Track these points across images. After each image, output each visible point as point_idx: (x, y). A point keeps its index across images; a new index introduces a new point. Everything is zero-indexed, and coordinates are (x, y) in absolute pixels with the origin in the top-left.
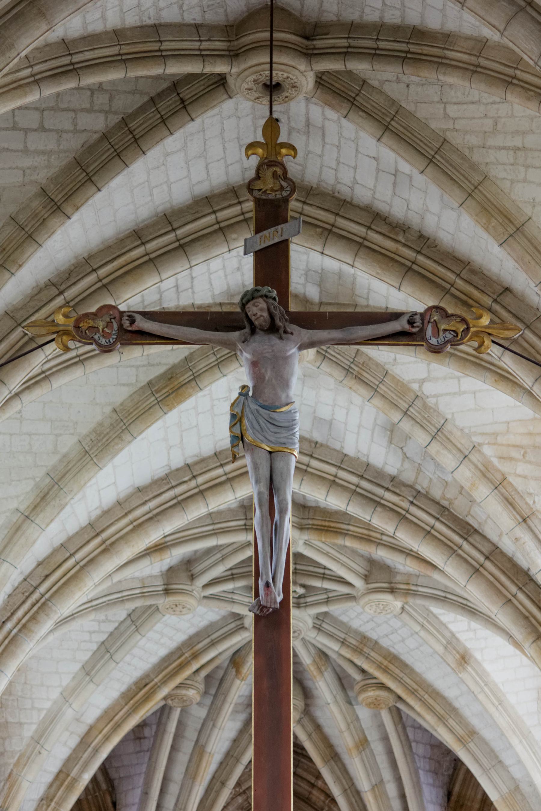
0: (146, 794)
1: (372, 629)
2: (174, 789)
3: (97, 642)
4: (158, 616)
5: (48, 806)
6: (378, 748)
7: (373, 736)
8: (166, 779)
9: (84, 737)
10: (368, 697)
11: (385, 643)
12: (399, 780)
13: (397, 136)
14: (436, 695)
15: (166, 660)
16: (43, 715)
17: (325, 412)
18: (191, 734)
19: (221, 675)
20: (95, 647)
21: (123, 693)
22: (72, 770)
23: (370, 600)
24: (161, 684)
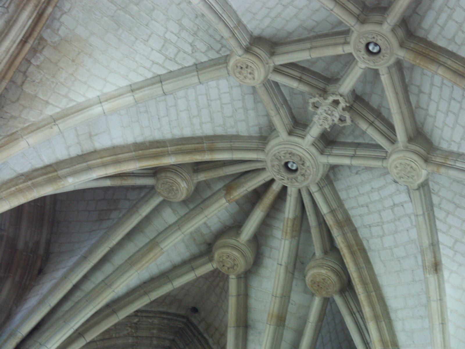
1: (361, 216)
2: (108, 269)
3: (154, 73)
4: (224, 72)
5: (24, 182)
9: (85, 154)
10: (319, 274)
11: (363, 233)
16: (71, 105)
18: (150, 233)
19: (207, 196)
20: (150, 75)
21: (136, 143)
22: (61, 169)
23: (404, 156)
24: (172, 154)
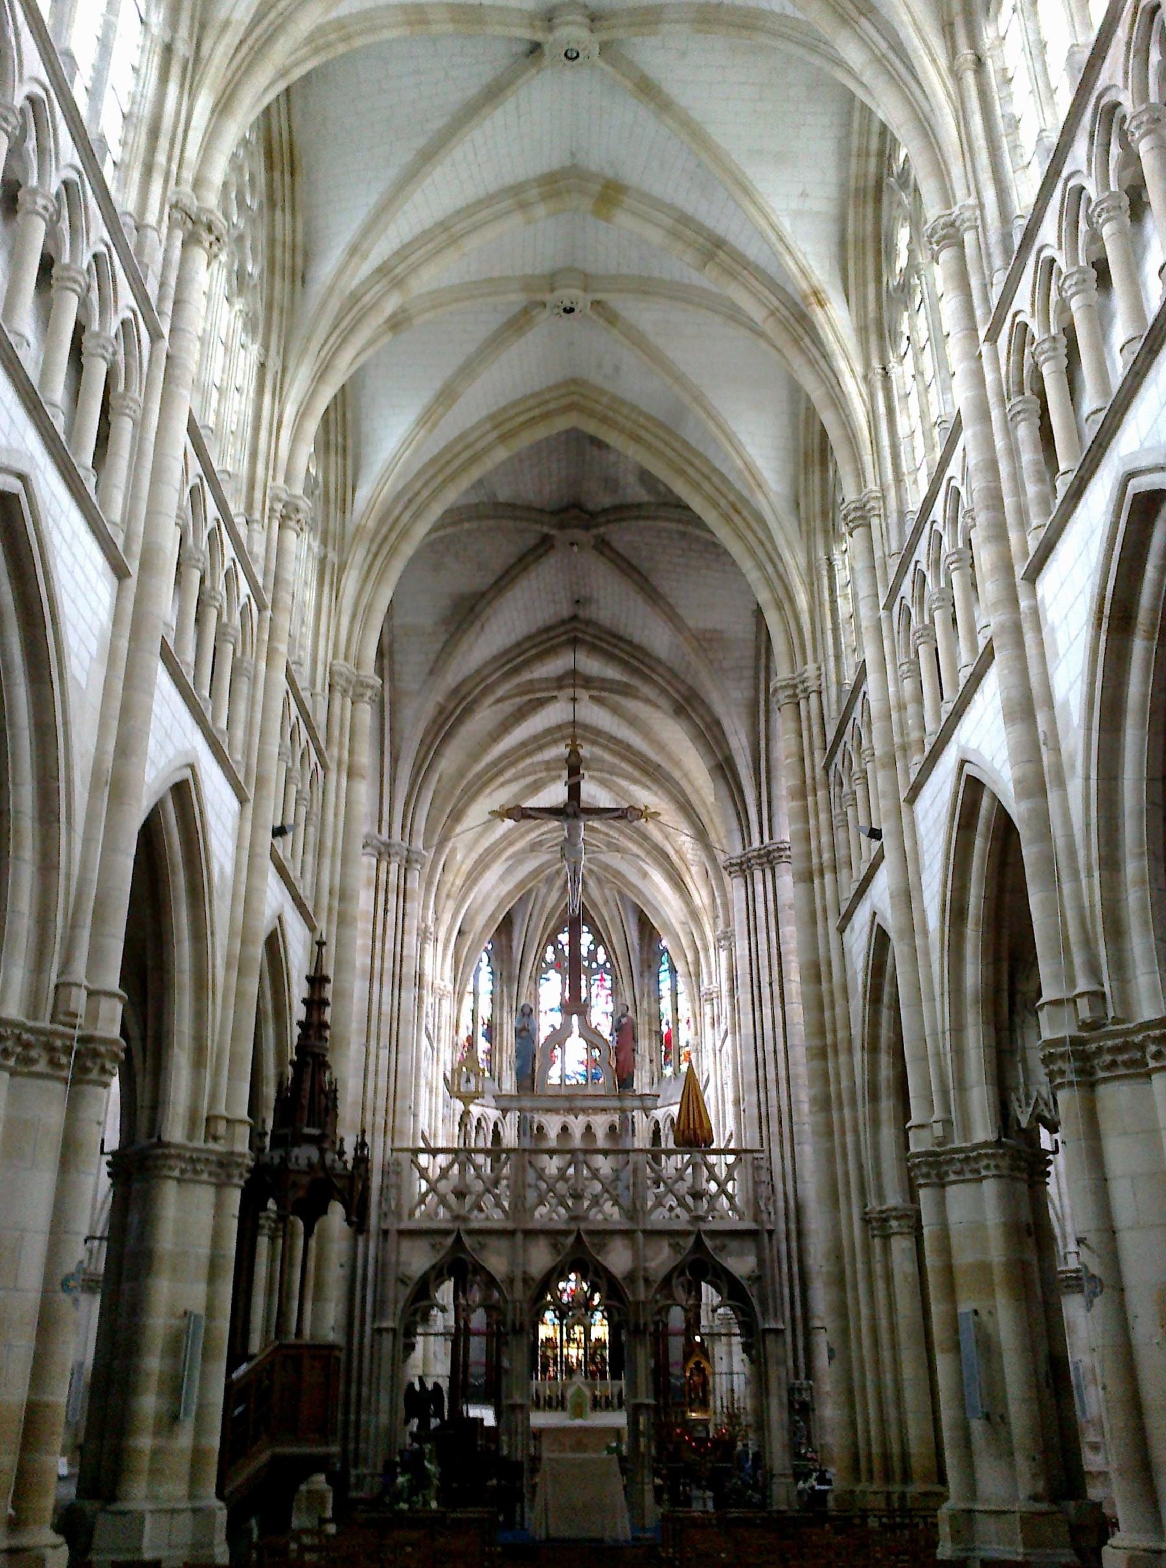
0: (523, 920)
6: (612, 904)
14: (635, 887)
15: (531, 873)
17: (593, 793)
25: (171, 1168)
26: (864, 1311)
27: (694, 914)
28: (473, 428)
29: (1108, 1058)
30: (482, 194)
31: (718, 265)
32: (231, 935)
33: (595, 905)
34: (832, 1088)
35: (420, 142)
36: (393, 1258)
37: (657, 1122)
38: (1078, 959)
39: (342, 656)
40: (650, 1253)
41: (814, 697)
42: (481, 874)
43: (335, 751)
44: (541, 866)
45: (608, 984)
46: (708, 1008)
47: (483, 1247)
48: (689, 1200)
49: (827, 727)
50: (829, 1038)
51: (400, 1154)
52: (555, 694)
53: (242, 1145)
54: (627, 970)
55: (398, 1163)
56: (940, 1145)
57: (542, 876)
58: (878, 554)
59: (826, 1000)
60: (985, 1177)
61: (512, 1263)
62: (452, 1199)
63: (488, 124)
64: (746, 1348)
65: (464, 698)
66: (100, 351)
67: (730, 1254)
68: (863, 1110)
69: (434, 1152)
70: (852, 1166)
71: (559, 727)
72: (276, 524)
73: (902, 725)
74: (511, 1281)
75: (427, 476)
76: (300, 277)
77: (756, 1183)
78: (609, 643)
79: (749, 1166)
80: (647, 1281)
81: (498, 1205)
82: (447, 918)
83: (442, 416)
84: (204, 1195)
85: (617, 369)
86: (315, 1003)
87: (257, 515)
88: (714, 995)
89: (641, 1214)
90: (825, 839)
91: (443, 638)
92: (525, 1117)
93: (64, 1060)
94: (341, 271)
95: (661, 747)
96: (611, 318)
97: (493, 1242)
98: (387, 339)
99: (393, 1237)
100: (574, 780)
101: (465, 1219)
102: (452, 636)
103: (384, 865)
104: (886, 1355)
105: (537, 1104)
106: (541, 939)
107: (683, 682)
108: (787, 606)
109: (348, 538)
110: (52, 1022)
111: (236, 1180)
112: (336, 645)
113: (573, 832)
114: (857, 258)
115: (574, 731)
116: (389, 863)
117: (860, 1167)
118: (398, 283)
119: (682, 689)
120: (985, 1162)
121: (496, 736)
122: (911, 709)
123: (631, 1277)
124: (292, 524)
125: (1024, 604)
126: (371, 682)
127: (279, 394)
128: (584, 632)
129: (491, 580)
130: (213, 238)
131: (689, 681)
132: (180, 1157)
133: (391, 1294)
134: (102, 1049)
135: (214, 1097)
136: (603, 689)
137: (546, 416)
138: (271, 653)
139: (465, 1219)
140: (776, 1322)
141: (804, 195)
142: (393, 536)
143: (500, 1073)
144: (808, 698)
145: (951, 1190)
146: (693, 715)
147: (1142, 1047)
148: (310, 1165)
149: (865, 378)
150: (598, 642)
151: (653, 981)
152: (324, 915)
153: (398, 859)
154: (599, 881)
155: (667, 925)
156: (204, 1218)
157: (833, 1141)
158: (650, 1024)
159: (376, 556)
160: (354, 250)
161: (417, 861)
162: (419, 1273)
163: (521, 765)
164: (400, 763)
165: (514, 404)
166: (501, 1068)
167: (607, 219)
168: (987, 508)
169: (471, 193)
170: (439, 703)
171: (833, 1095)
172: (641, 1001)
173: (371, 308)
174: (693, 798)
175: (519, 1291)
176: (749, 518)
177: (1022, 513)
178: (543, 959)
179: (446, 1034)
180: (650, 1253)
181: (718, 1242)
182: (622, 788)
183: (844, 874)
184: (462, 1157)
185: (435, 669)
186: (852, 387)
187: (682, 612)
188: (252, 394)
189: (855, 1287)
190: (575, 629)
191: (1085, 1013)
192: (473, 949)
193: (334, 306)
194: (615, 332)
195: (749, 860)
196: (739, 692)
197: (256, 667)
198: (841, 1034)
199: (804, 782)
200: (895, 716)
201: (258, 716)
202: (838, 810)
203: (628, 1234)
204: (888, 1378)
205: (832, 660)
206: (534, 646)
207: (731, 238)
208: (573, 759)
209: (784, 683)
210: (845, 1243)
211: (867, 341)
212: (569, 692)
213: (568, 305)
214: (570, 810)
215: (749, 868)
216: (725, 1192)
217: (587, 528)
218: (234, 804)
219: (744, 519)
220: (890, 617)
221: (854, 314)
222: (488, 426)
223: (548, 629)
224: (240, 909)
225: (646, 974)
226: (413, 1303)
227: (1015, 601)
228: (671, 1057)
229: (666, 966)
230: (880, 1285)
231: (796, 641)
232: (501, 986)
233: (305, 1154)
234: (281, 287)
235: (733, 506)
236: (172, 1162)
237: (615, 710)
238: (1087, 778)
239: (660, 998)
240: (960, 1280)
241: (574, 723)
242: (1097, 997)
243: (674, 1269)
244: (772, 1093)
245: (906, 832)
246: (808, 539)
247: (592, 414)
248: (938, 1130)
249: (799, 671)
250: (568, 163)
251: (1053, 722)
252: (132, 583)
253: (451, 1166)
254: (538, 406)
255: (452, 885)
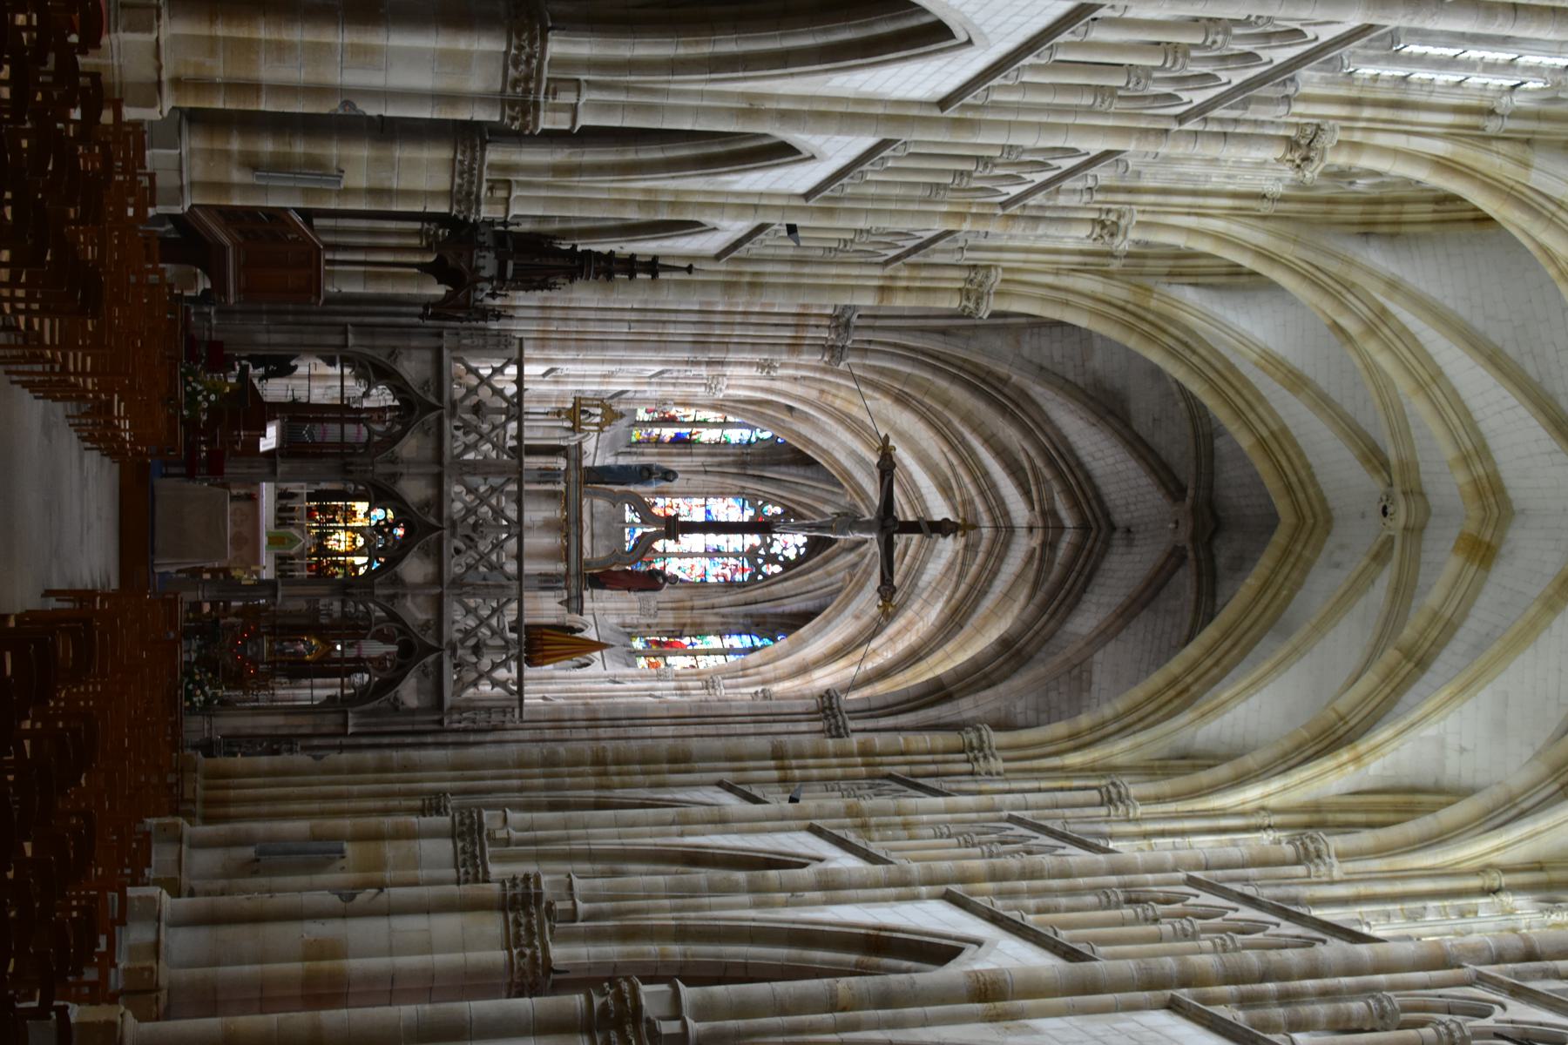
0: (808, 478)
2: (811, 491)
6: (828, 581)
7: (832, 579)
8: (815, 488)
12: (815, 590)
13: (1015, 581)
15: (860, 487)
25: (463, 153)
26: (356, 788)
27: (804, 670)
28: (1272, 412)
29: (523, 920)
30: (1477, 416)
31: (1399, 663)
32: (677, 192)
33: (827, 561)
34: (566, 770)
35: (1511, 350)
36: (415, 343)
37: (581, 630)
38: (605, 905)
39: (1008, 276)
40: (420, 600)
41: (967, 767)
42: (848, 428)
43: (905, 273)
44: (868, 497)
45: (738, 577)
46: (699, 684)
47: (426, 433)
48: (471, 642)
49: (933, 779)
50: (613, 768)
51: (516, 347)
52: (1037, 508)
53: (486, 212)
54: (753, 599)
55: (507, 345)
56: (488, 835)
57: (858, 499)
58: (1068, 812)
59: (652, 767)
60: (458, 872)
61: (409, 463)
62: (473, 400)
63: (1533, 422)
64: (331, 699)
65: (1018, 405)
66: (1134, 80)
67: (419, 682)
68: (543, 797)
69: (519, 381)
70: (489, 783)
71: (1006, 514)
72: (1094, 215)
73: (887, 826)
74: (394, 461)
75: (1213, 361)
76: (1367, 231)
77: (489, 710)
78: (1083, 566)
79: (505, 703)
80: (392, 597)
81: (467, 448)
82: (798, 390)
83: (1272, 376)
84: (442, 181)
85: (1337, 565)
86: (631, 266)
87: (1098, 197)
88: (711, 691)
89: (458, 591)
90: (815, 772)
91: (1080, 382)
92: (559, 476)
93: (519, 90)
94: (1371, 273)
95: (979, 630)
96: (1380, 556)
97: (430, 444)
98: (1328, 322)
99: (433, 342)
100: (924, 527)
101: (453, 415)
102: (1083, 391)
103: (826, 322)
104: (315, 806)
105: (572, 486)
106: (791, 500)
107: (1039, 649)
108: (1071, 743)
109: (1136, 280)
110: (548, 79)
111: (455, 208)
112: (1019, 270)
113: (866, 527)
114: (1395, 805)
115: (1005, 529)
116: (829, 327)
117: (489, 791)
118: (1371, 330)
119: (1029, 649)
120: (471, 870)
121: (991, 442)
122: (905, 833)
123: (397, 581)
124: (1098, 230)
125: (924, 890)
126: (983, 307)
127: (1234, 214)
128: (1096, 540)
129: (1143, 433)
130: (1298, 161)
131: (1040, 655)
132: (473, 159)
133: (379, 342)
134: (530, 118)
135: (529, 185)
136: (1041, 560)
137: (1289, 489)
138: (962, 216)
139: (453, 415)
140: (355, 725)
141: (1462, 750)
142: (1146, 327)
143: (635, 454)
144: (968, 761)
145: (449, 844)
146: (1001, 659)
147: (530, 945)
148: (479, 269)
149: (1263, 808)
150: (1085, 553)
151: (741, 628)
152: (731, 268)
153: (833, 336)
154: (854, 565)
155: (803, 643)
156: (422, 182)
157: (514, 767)
158: (693, 625)
159: (1123, 309)
160: (1393, 285)
161: (832, 357)
162: (401, 370)
163: (961, 471)
164: (941, 338)
165: (1301, 454)
166: (643, 454)
167: (1455, 550)
168: (1023, 868)
169: (1474, 404)
170: (1010, 378)
171: (556, 769)
172: (717, 614)
173: (1342, 303)
174: (923, 665)
175: (382, 469)
176: (1171, 707)
177: (1013, 894)
178: (766, 503)
179: (678, 392)
180: (420, 600)
181: (430, 669)
182: (945, 588)
183: (777, 788)
184: (513, 410)
185: (1044, 373)
186: (1251, 795)
187: (1111, 646)
188: (1230, 187)
189: (377, 782)
190: (1099, 529)
191: (559, 906)
192: (771, 423)
193: (1333, 267)
194: (1365, 561)
195: (835, 717)
196: (1021, 708)
197: (942, 202)
198: (616, 779)
199: (879, 755)
200: (898, 819)
201: (892, 206)
202: (843, 786)
203: (438, 579)
204: (295, 807)
205: (1006, 786)
206: (1079, 484)
207: (1427, 676)
208: (949, 526)
209: (985, 738)
210: (418, 775)
211: (1304, 812)
212: (1040, 523)
213: (1390, 510)
214: (889, 522)
215: (826, 717)
216: (481, 676)
217: (1194, 538)
218: (803, 186)
219: (1170, 701)
220: (1000, 820)
221: (1335, 800)
222: (1275, 428)
223: (1099, 497)
224: (701, 199)
225: (749, 621)
226: (370, 363)
227: (930, 882)
228: (654, 647)
229: (758, 643)
230: (379, 804)
231: (1030, 752)
232: (734, 455)
233: (488, 264)
234: (1353, 212)
235: (1186, 690)
236: (468, 153)
237: (1019, 576)
238: (754, 920)
239: (721, 635)
240: (372, 845)
241: (1011, 529)
242: (572, 916)
243: (405, 624)
244: (584, 734)
245: (781, 822)
246: (1145, 767)
247: (1293, 539)
248: (501, 834)
249: (997, 753)
250: (1516, 506)
251: (813, 903)
252: (937, 113)
253: (505, 398)
254: (1301, 482)
255: (835, 396)
